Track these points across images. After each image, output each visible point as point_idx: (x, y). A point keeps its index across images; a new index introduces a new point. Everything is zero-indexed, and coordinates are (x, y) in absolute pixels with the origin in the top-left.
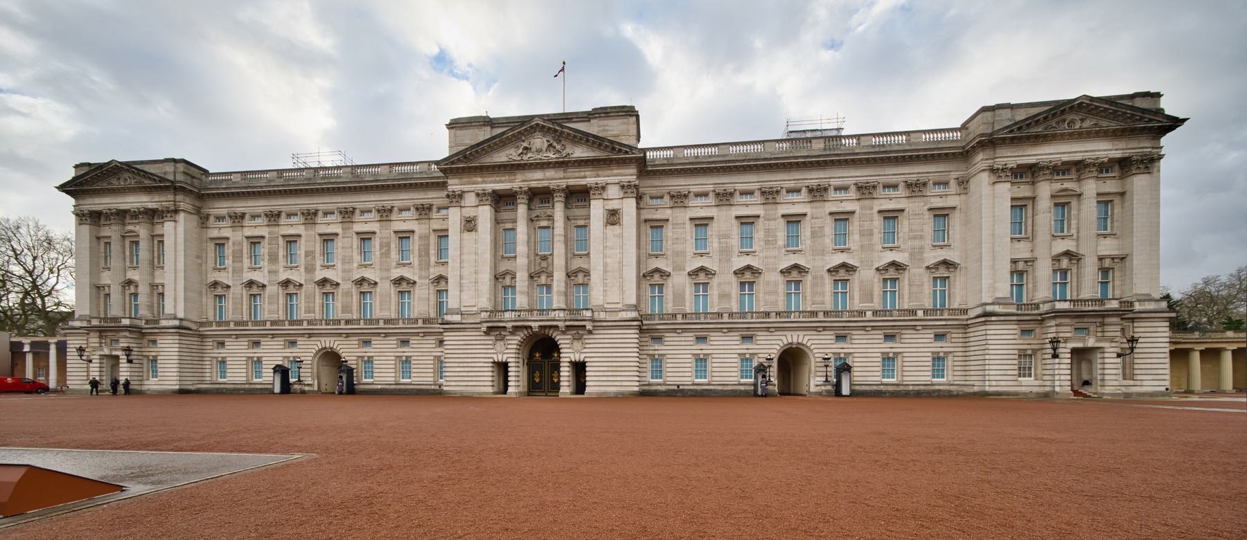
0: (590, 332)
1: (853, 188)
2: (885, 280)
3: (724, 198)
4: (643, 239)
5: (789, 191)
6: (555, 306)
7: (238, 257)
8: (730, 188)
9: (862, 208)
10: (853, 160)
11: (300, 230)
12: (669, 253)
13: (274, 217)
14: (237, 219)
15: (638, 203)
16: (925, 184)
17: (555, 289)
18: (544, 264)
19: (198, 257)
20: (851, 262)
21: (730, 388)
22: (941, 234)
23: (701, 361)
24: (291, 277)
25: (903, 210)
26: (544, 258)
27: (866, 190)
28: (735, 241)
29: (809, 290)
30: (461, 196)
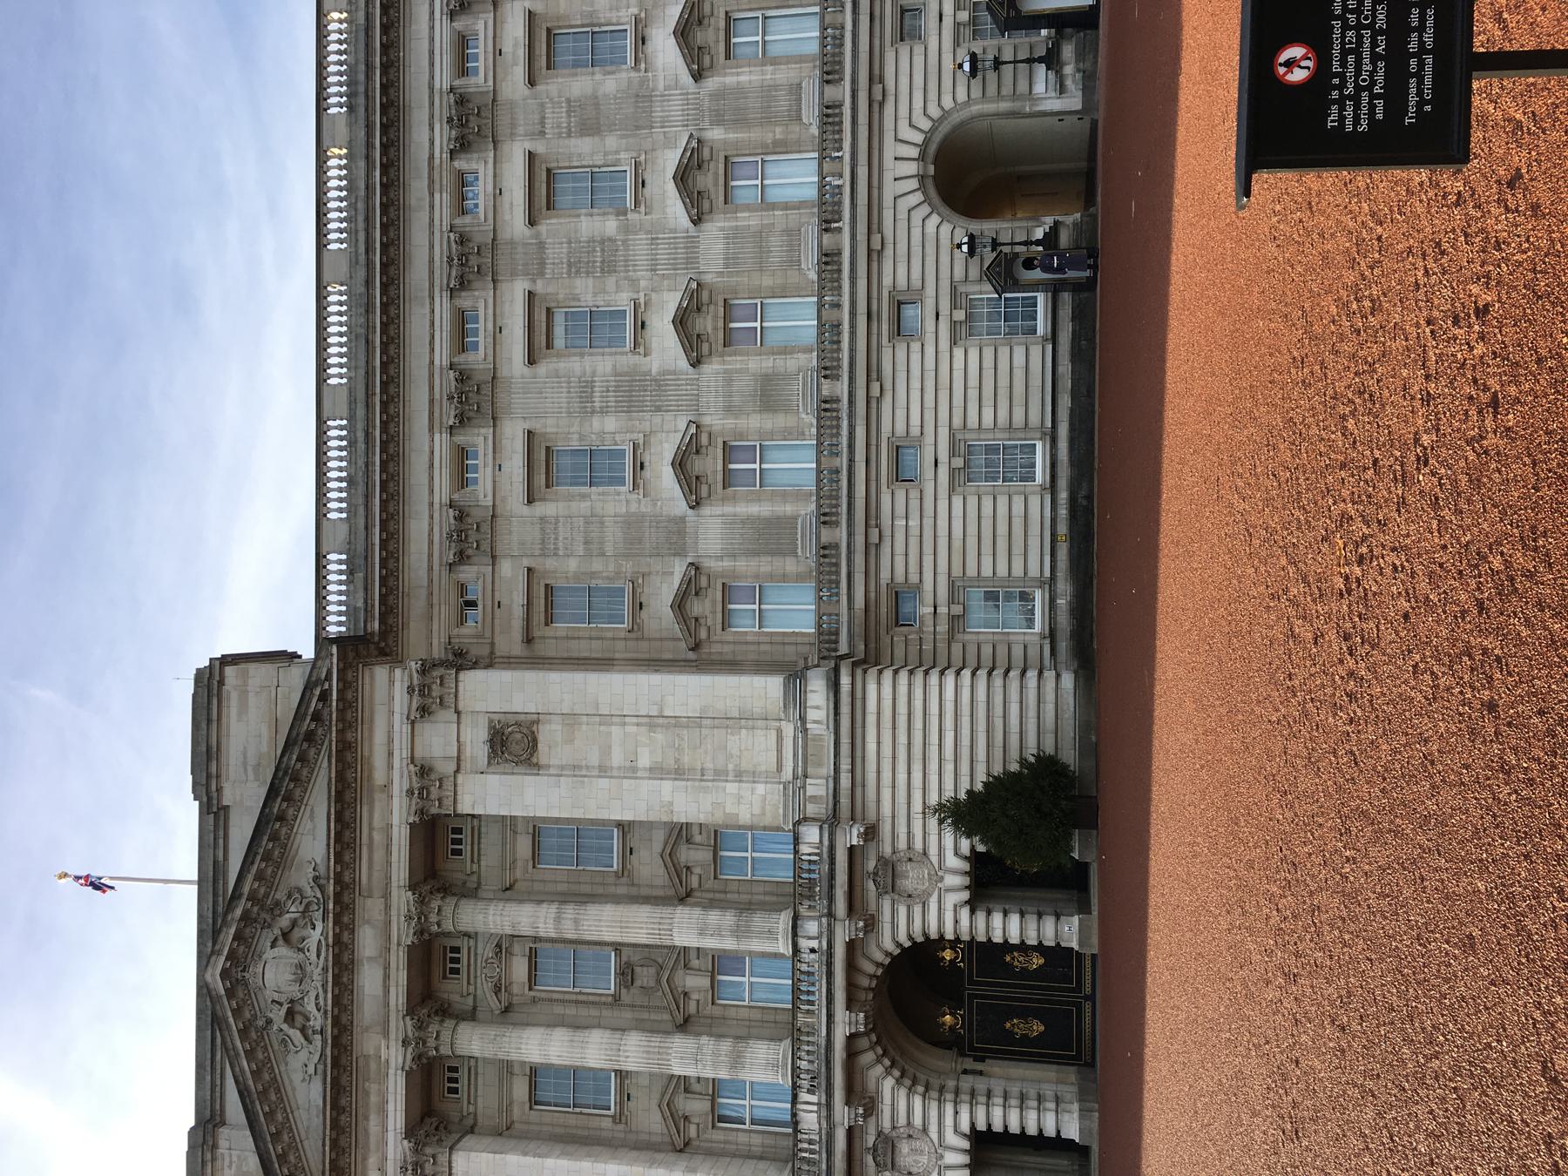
0: (871, 833)
1: (459, 25)
3: (472, 399)
4: (582, 649)
5: (461, 205)
6: (784, 947)
10: (385, 29)
12: (628, 567)
15: (475, 665)
17: (729, 944)
18: (645, 976)
21: (1065, 367)
23: (976, 462)
26: (627, 974)
28: (602, 364)
29: (755, 135)
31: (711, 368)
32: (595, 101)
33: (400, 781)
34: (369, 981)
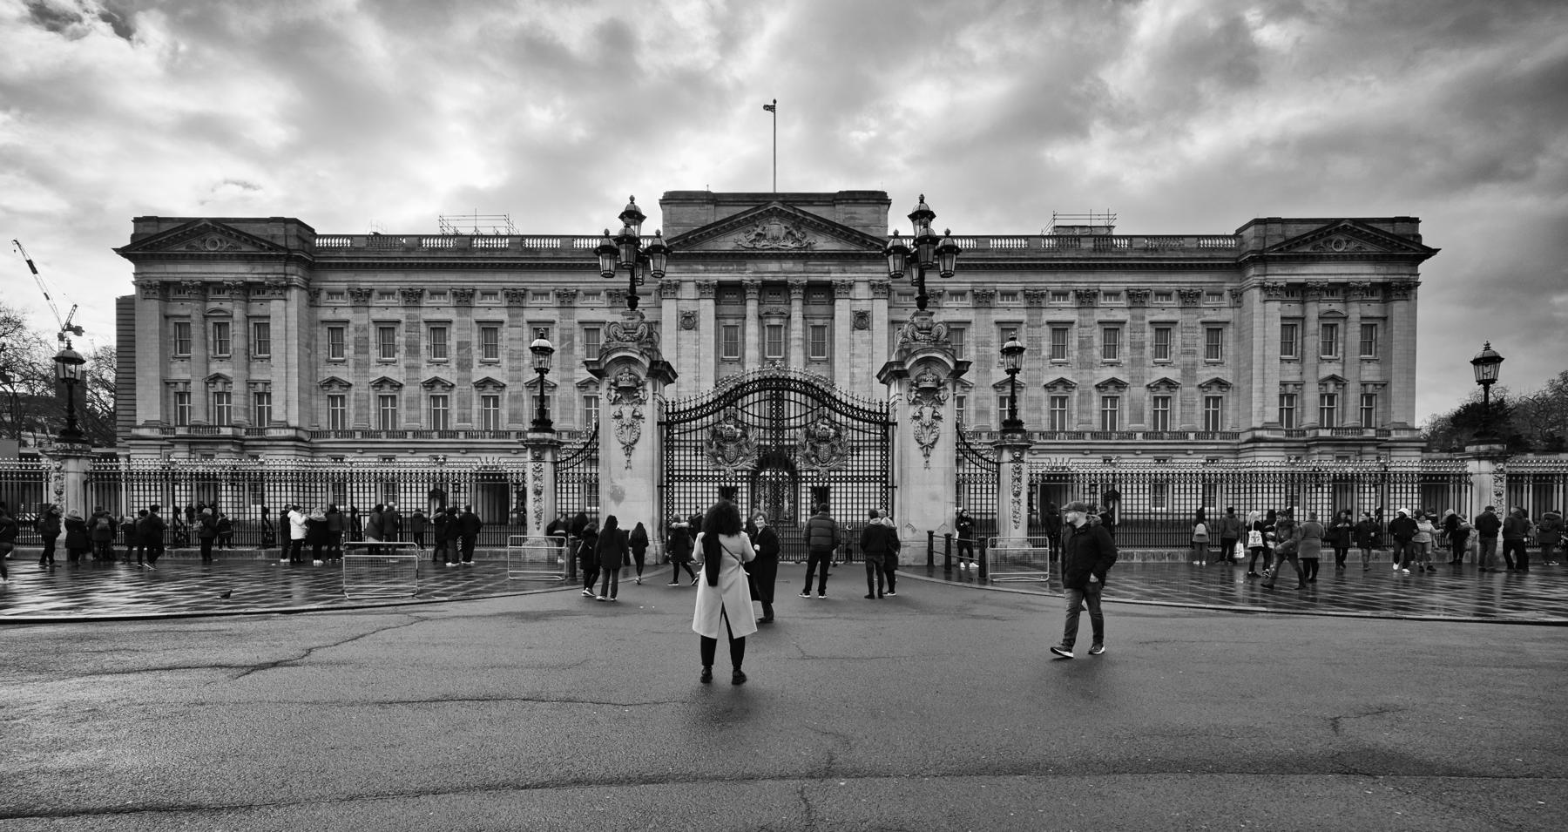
1: (1124, 294)
2: (1156, 399)
3: (983, 299)
7: (362, 347)
8: (989, 288)
9: (1133, 317)
11: (451, 315)
13: (413, 297)
14: (361, 297)
16: (1198, 295)
19: (308, 346)
20: (1121, 377)
22: (1214, 348)
24: (439, 375)
25: (1175, 323)
27: (1137, 298)
30: (677, 286)
31: (993, 393)
32: (1091, 348)
33: (848, 277)
34: (773, 266)
